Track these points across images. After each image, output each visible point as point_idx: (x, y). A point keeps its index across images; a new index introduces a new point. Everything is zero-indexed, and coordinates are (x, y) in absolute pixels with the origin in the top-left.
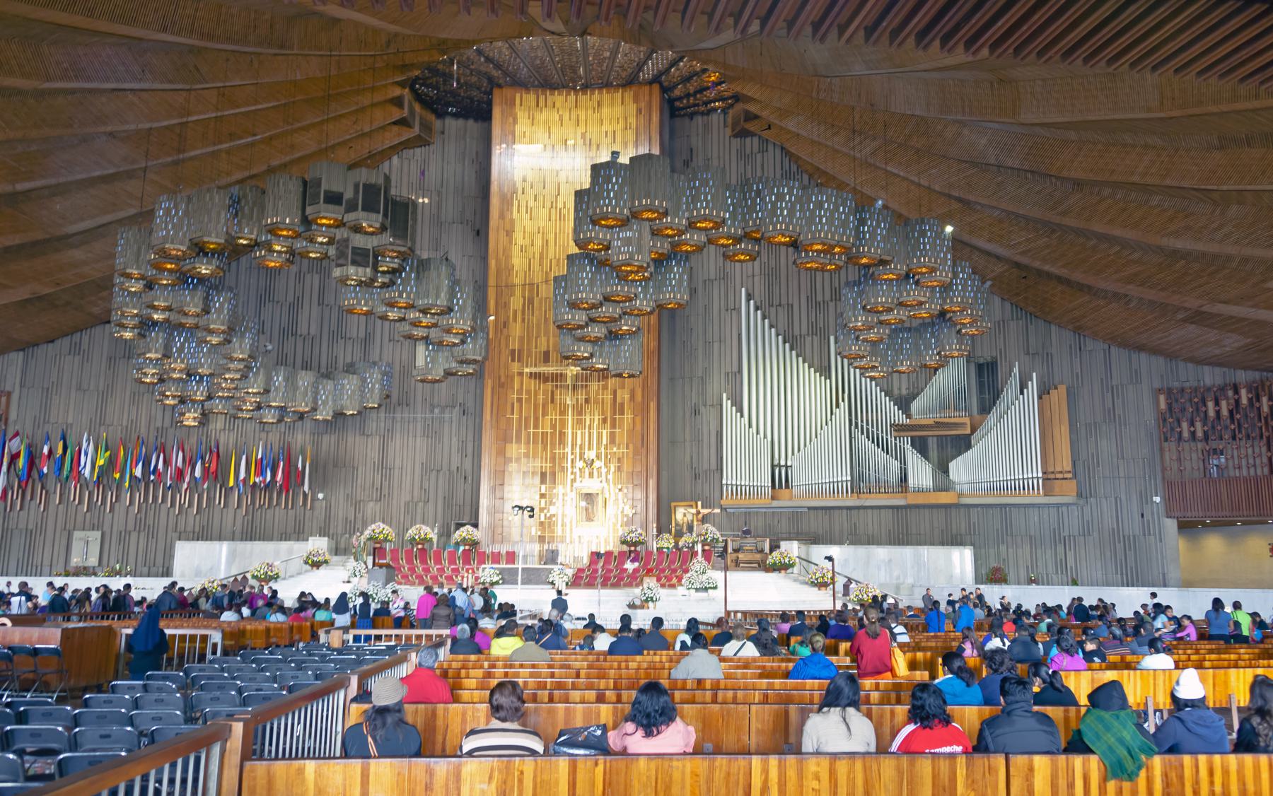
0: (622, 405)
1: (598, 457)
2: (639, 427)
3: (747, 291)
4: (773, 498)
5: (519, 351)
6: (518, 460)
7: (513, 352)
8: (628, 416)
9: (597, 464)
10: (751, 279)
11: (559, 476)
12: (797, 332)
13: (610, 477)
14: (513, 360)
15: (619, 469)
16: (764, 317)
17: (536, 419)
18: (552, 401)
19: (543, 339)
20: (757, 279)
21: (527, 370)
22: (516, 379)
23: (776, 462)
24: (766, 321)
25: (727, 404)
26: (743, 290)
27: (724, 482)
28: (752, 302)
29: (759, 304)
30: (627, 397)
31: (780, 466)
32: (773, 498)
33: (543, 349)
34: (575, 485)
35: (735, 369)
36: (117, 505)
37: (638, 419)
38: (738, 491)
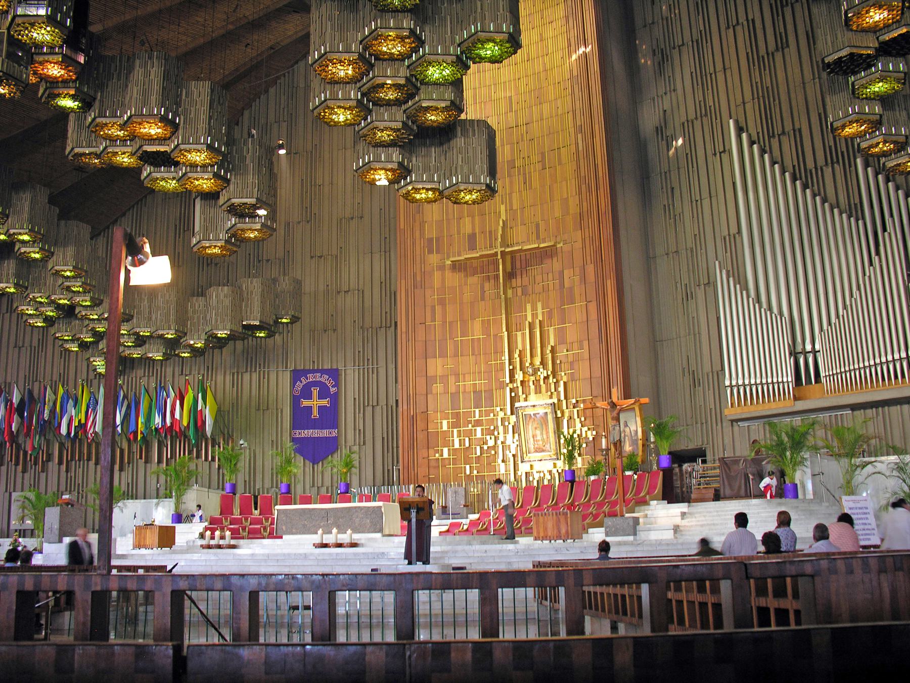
0: (571, 289)
1: (542, 363)
2: (593, 316)
3: (737, 122)
4: (796, 399)
5: (438, 239)
6: (444, 379)
7: (430, 240)
8: (579, 304)
9: (542, 373)
10: (741, 109)
11: (496, 394)
12: (810, 165)
13: (561, 389)
14: (431, 251)
15: (572, 377)
16: (763, 152)
17: (464, 323)
18: (483, 299)
19: (467, 220)
20: (749, 106)
21: (448, 262)
22: (437, 275)
23: (799, 348)
24: (766, 156)
25: (720, 276)
26: (731, 122)
27: (727, 383)
28: (744, 136)
29: (755, 138)
30: (577, 278)
31: (805, 353)
32: (796, 399)
33: (467, 229)
34: (517, 405)
35: (734, 230)
36: (50, 464)
37: (593, 307)
38: (747, 395)
